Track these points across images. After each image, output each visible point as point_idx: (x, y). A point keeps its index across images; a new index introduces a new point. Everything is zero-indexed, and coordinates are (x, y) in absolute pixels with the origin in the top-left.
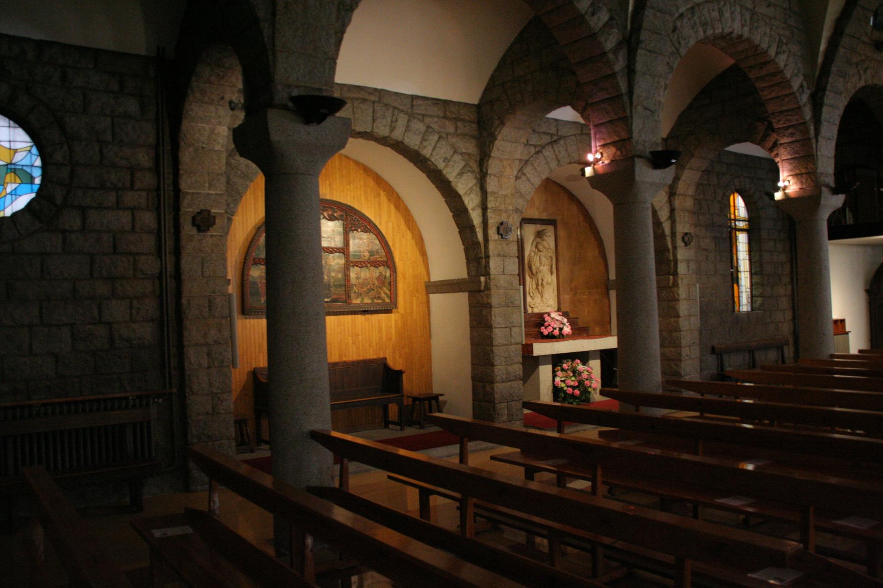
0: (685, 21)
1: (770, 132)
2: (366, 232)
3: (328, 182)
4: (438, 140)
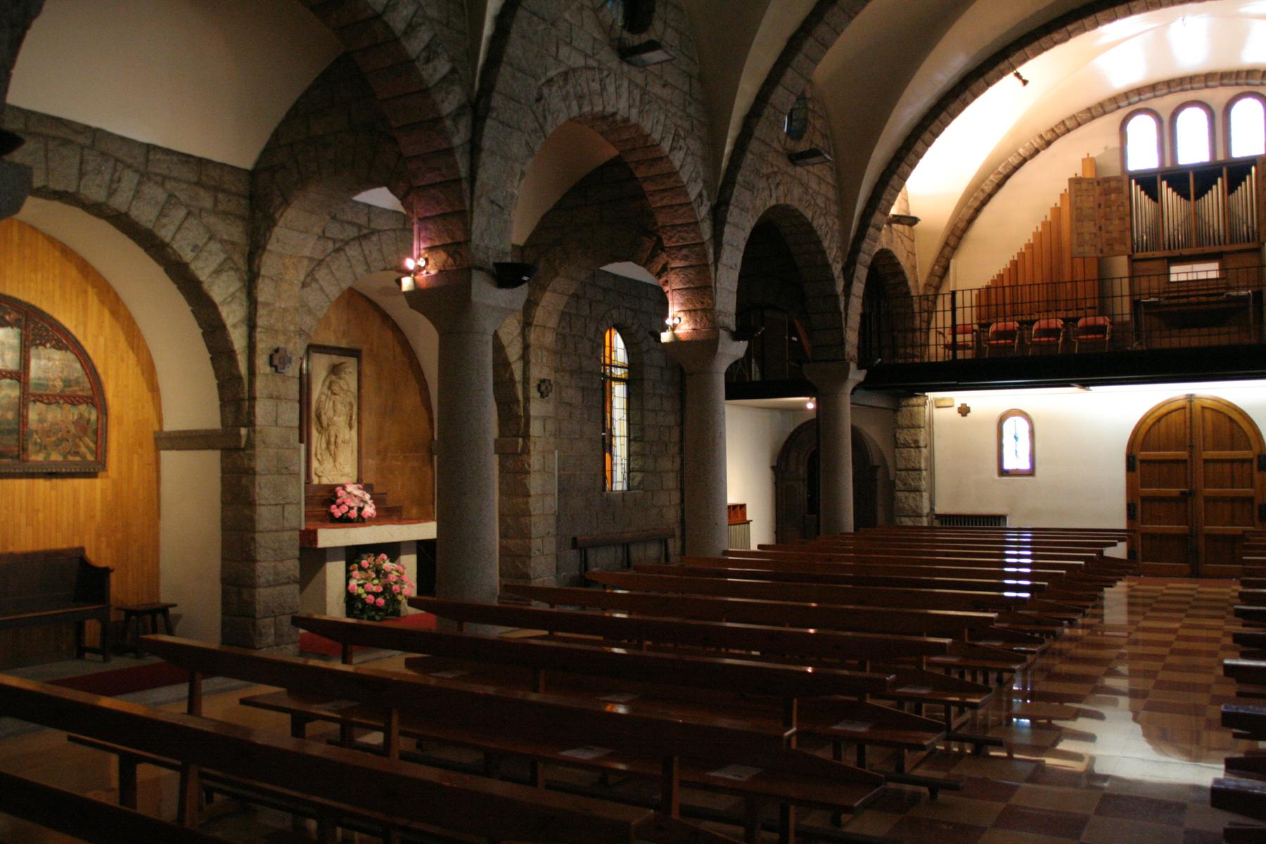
0: (555, 88)
1: (659, 252)
2: (60, 349)
4: (186, 218)
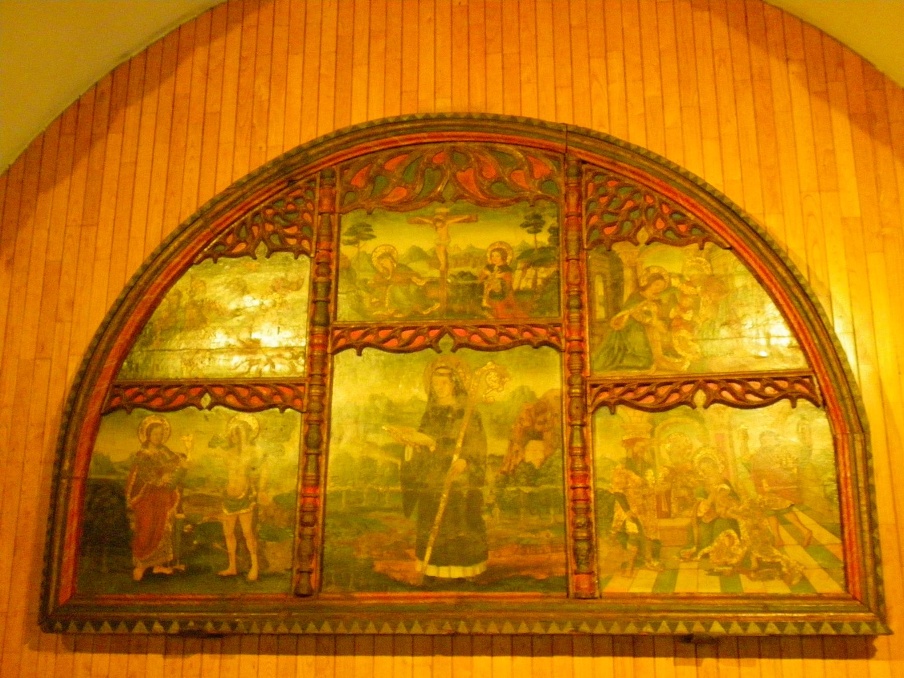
2: (681, 241)
3: (495, 59)
